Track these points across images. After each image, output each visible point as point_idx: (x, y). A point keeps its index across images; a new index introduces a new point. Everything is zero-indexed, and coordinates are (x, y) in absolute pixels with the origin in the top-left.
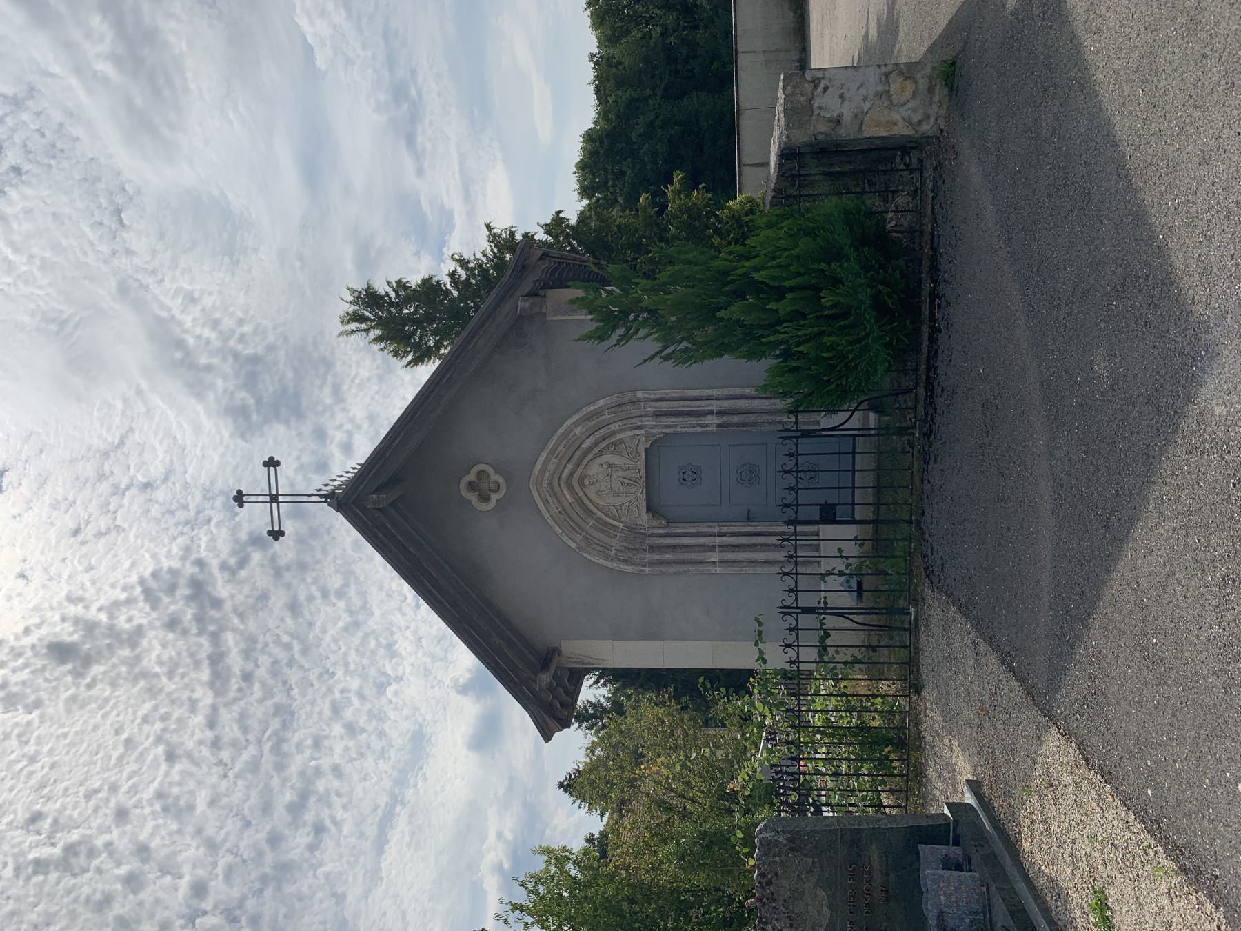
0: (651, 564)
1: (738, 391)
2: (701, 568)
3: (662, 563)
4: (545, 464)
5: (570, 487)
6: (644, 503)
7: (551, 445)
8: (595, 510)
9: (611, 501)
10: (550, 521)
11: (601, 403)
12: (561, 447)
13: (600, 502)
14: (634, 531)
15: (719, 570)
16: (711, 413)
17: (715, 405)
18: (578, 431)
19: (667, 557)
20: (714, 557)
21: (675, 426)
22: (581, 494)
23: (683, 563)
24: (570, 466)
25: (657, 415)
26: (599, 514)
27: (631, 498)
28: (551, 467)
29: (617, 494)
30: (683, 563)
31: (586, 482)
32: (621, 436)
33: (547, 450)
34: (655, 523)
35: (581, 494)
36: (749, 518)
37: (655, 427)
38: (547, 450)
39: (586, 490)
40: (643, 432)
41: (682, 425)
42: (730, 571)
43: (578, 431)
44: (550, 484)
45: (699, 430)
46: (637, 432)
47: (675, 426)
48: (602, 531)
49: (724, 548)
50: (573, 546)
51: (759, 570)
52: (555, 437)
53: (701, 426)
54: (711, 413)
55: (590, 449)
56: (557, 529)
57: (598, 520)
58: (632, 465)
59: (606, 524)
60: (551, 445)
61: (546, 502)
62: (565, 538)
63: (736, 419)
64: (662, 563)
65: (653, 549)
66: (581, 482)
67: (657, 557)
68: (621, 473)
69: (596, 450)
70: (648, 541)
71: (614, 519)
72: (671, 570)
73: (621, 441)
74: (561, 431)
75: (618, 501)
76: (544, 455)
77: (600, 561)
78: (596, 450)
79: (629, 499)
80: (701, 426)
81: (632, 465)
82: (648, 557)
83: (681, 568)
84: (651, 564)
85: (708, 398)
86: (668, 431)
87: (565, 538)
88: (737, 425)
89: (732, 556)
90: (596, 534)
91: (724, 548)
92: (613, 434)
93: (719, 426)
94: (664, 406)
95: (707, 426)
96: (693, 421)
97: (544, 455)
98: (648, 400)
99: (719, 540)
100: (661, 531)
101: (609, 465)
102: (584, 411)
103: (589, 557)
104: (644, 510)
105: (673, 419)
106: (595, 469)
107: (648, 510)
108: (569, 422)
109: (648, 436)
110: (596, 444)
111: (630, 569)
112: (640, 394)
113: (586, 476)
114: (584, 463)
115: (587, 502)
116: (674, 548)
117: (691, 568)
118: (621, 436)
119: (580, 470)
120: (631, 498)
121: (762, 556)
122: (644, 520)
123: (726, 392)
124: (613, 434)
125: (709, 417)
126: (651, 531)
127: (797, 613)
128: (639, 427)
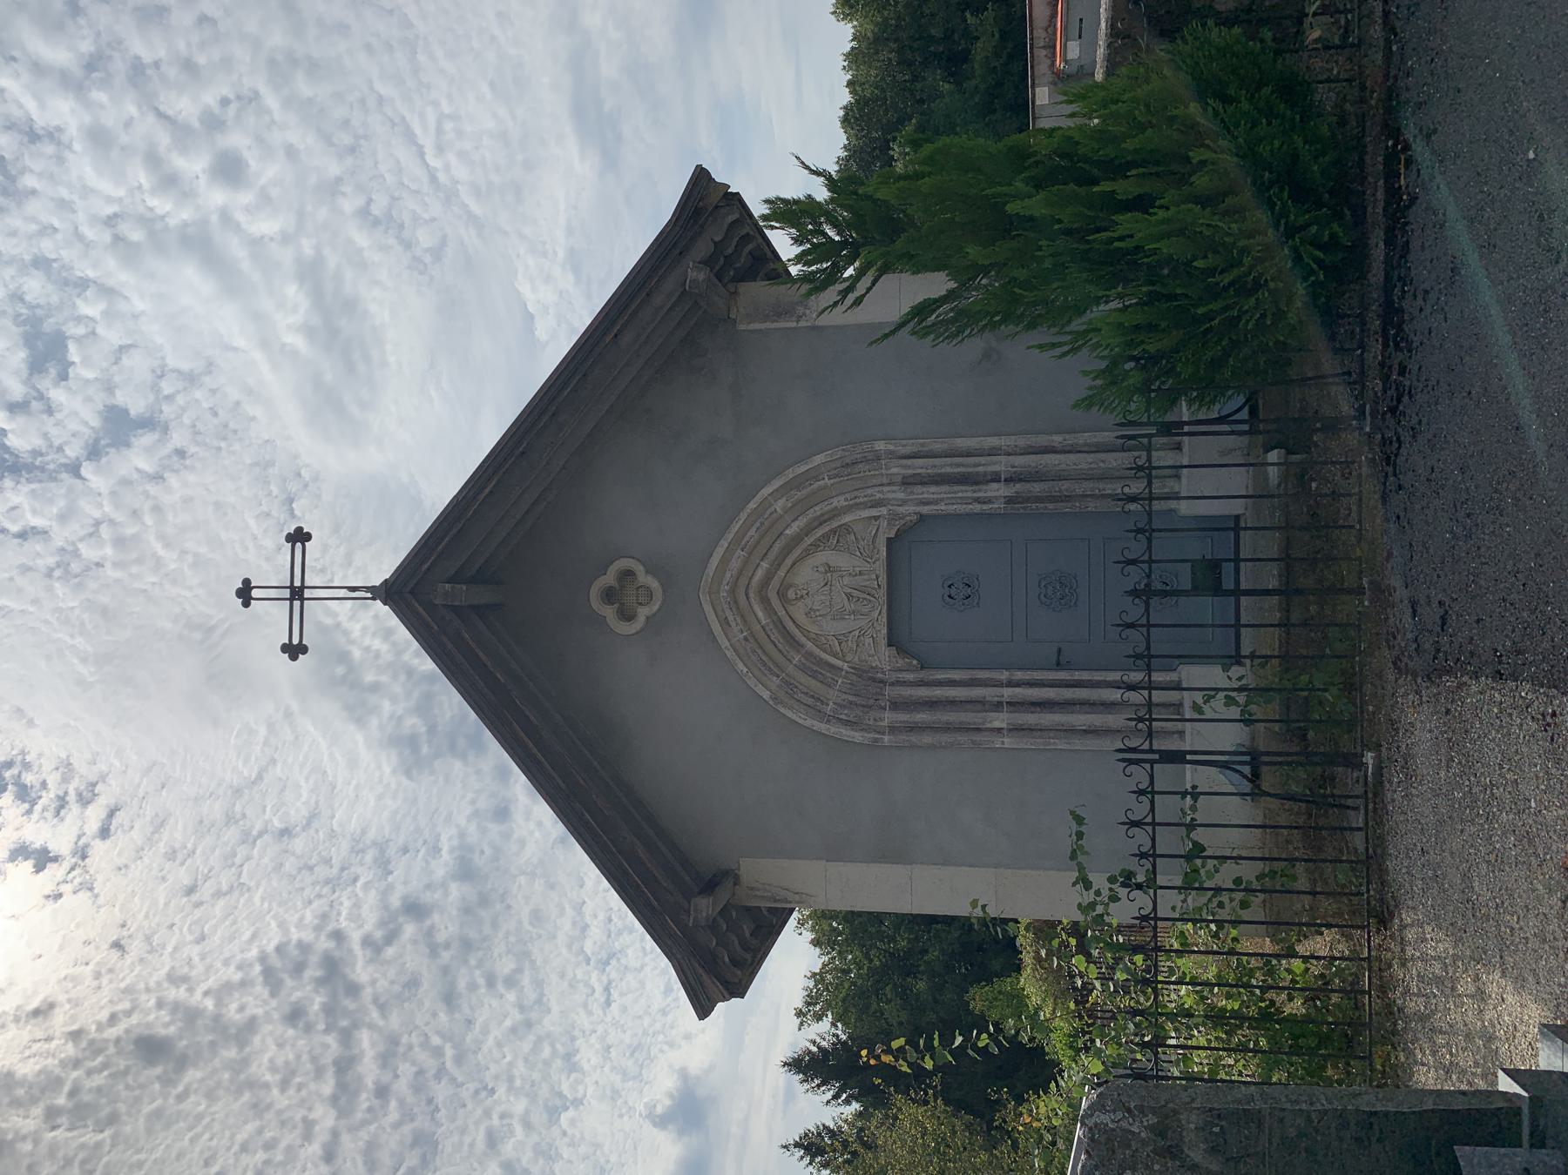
0: (893, 729)
1: (1042, 440)
2: (977, 737)
3: (912, 728)
4: (725, 561)
5: (765, 601)
6: (884, 631)
7: (736, 527)
8: (803, 640)
9: (830, 627)
10: (730, 653)
11: (818, 459)
12: (752, 532)
13: (813, 629)
14: (866, 677)
15: (1008, 742)
16: (996, 478)
17: (1001, 465)
18: (779, 505)
19: (921, 717)
20: (999, 720)
21: (936, 502)
22: (782, 613)
23: (948, 728)
24: (765, 565)
25: (907, 482)
26: (809, 645)
28: (735, 564)
30: (948, 728)
31: (791, 594)
32: (847, 519)
33: (730, 536)
34: (901, 663)
35: (782, 613)
36: (1059, 665)
37: (904, 502)
38: (730, 536)
39: (790, 608)
40: (884, 511)
41: (948, 500)
42: (1025, 743)
43: (779, 505)
44: (733, 592)
45: (977, 508)
46: (874, 512)
47: (936, 502)
49: (1015, 705)
50: (766, 695)
51: (1078, 744)
52: (743, 516)
53: (978, 500)
54: (996, 478)
55: (798, 539)
56: (741, 666)
57: (809, 655)
60: (736, 527)
61: (725, 623)
63: (1037, 488)
64: (912, 728)
65: (895, 706)
66: (782, 595)
67: (904, 717)
68: (846, 581)
69: (809, 540)
70: (887, 690)
72: (927, 739)
73: (847, 528)
74: (752, 505)
76: (724, 543)
77: (809, 723)
78: (809, 540)
80: (978, 500)
82: (888, 717)
83: (945, 738)
84: (893, 729)
85: (993, 452)
86: (925, 510)
87: (752, 682)
88: (1039, 499)
89: (1030, 719)
90: (804, 679)
91: (1015, 705)
92: (836, 513)
93: (1010, 500)
94: (920, 466)
95: (989, 501)
96: (967, 492)
97: (724, 543)
98: (892, 455)
99: (1008, 693)
100: (910, 677)
101: (829, 569)
103: (789, 714)
104: (884, 642)
105: (933, 489)
106: (806, 575)
107: (890, 645)
108: (766, 491)
109: (893, 517)
110: (807, 530)
111: (858, 736)
112: (880, 446)
114: (789, 561)
116: (932, 704)
117: (962, 738)
118: (847, 519)
119: (781, 573)
121: (1081, 720)
122: (882, 658)
123: (1022, 442)
124: (836, 513)
125: (994, 485)
126: (894, 676)
127: (1152, 762)
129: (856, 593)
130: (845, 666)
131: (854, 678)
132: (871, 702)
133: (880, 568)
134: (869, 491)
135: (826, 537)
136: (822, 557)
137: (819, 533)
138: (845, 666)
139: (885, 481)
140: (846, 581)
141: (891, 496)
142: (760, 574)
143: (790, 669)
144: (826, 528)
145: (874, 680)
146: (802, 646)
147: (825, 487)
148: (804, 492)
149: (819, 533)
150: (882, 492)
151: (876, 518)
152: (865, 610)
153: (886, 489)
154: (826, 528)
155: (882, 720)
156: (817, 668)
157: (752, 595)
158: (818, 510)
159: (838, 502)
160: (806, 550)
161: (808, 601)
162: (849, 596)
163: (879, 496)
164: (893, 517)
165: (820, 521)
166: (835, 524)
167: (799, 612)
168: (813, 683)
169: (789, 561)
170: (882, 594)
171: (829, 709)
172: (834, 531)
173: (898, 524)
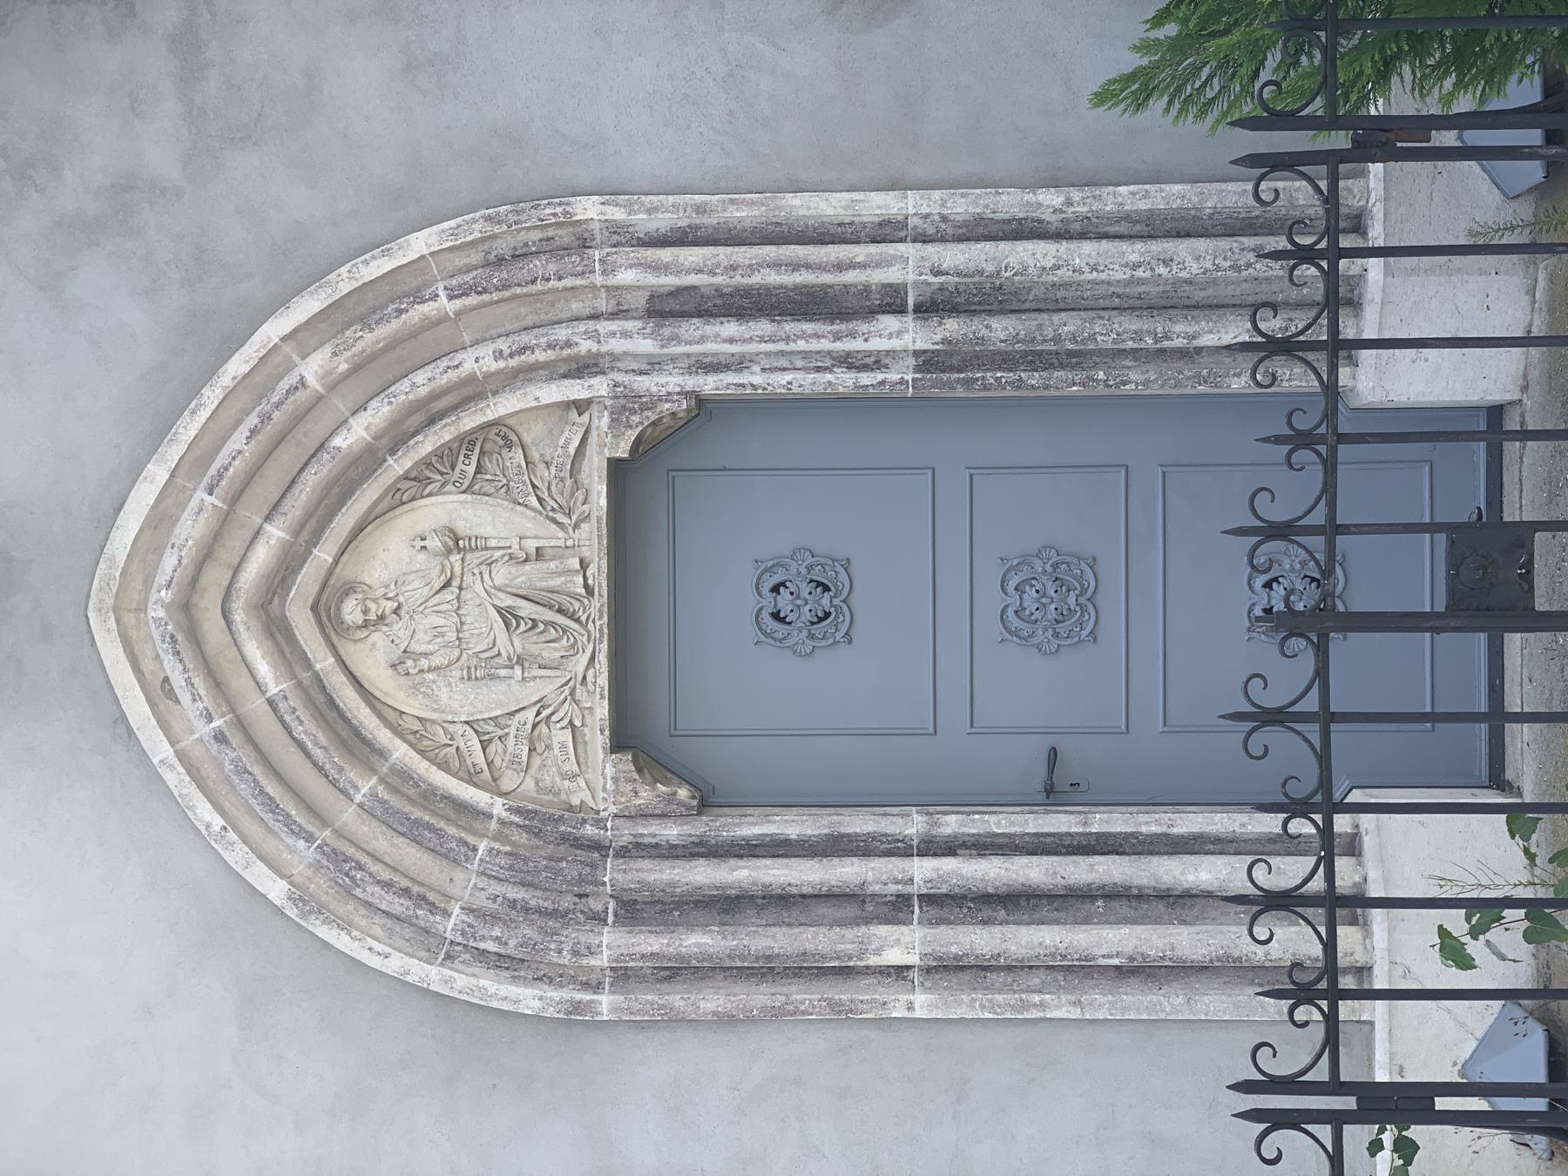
0: (623, 976)
1: (1009, 203)
2: (842, 993)
3: (673, 972)
4: (161, 520)
5: (278, 632)
6: (602, 710)
7: (189, 428)
8: (384, 736)
9: (457, 701)
10: (176, 778)
11: (420, 243)
12: (238, 440)
13: (413, 706)
15: (923, 1002)
16: (891, 302)
17: (905, 266)
18: (313, 368)
19: (697, 941)
20: (901, 945)
21: (739, 364)
22: (324, 662)
23: (765, 970)
24: (276, 533)
25: (666, 308)
26: (401, 752)
27: (545, 687)
28: (190, 529)
29: (485, 669)
30: (765, 970)
31: (351, 611)
32: (503, 406)
33: (173, 453)
34: (646, 796)
35: (324, 662)
36: (1053, 795)
37: (654, 364)
38: (173, 453)
39: (349, 651)
40: (599, 386)
41: (770, 361)
42: (968, 1004)
43: (313, 368)
44: (185, 608)
45: (844, 380)
46: (576, 390)
47: (739, 364)
48: (413, 832)
49: (946, 904)
50: (276, 890)
51: (1102, 1003)
52: (211, 396)
53: (849, 361)
54: (891, 302)
55: (368, 461)
56: (205, 813)
57: (402, 778)
58: (552, 537)
59: (430, 796)
60: (189, 428)
61: (160, 694)
62: (237, 856)
63: (1000, 330)
64: (673, 972)
65: (635, 910)
66: (325, 613)
67: (651, 943)
70: (613, 873)
72: (712, 1000)
73: (501, 434)
74: (237, 366)
75: (488, 700)
76: (158, 473)
79: (534, 691)
80: (849, 361)
81: (552, 537)
82: (611, 944)
83: (760, 996)
84: (623, 976)
85: (887, 232)
86: (709, 384)
87: (237, 856)
88: (1005, 360)
89: (979, 940)
90: (382, 841)
91: (946, 904)
92: (472, 391)
93: (928, 362)
94: (694, 267)
95: (877, 362)
96: (814, 337)
97: (158, 473)
98: (623, 237)
99: (923, 871)
100: (672, 832)
101: (455, 542)
102: (344, 282)
103: (341, 941)
104: (598, 740)
105: (731, 328)
106: (395, 557)
107: (618, 745)
108: (275, 329)
109: (625, 405)
110: (396, 437)
111: (529, 998)
112: (589, 209)
113: (349, 589)
115: (349, 698)
116: (728, 906)
117: (803, 995)
118: (503, 406)
119: (323, 554)
120: (545, 687)
121: (1111, 940)
122: (598, 782)
123: (961, 206)
124: (472, 391)
125: (889, 322)
126: (626, 834)
127: (1337, 1120)
128: (584, 368)
129: (526, 609)
130: (498, 807)
131: (521, 838)
132: (567, 902)
133: (592, 540)
134: (561, 333)
135: (447, 456)
136: (441, 509)
137: (426, 445)
138: (498, 807)
139: (603, 305)
140: (501, 574)
141: (616, 345)
142: (261, 558)
143: (348, 816)
144: (444, 433)
145: (577, 843)
146: (382, 754)
147: (442, 320)
148: (384, 332)
149: (426, 445)
150: (595, 336)
151: (581, 406)
152: (552, 653)
153: (604, 327)
154: (444, 433)
157: (239, 617)
158: (422, 382)
159: (479, 361)
161: (399, 629)
162: (509, 617)
163: (586, 346)
164: (625, 405)
165: (429, 413)
166: (470, 421)
168: (412, 857)
170: (597, 609)
171: (450, 926)
172: (467, 441)
173: (638, 423)
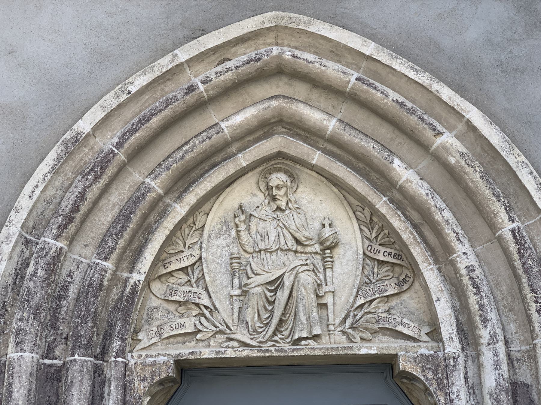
4: (338, 52)
5: (264, 128)
6: (207, 353)
7: (401, 65)
9: (215, 251)
10: (165, 63)
14: (110, 318)
22: (243, 160)
24: (331, 125)
26: (180, 210)
27: (226, 312)
28: (332, 70)
29: (237, 268)
32: (431, 276)
34: (140, 387)
35: (243, 160)
38: (384, 57)
40: (453, 346)
43: (449, 141)
44: (280, 71)
48: (123, 218)
50: (85, 125)
52: (424, 78)
55: (385, 183)
56: (140, 81)
57: (158, 209)
58: (335, 316)
59: (146, 231)
60: (401, 65)
62: (110, 101)
68: (307, 278)
69: (382, 205)
70: (81, 361)
71: (158, 261)
74: (446, 93)
75: (216, 272)
76: (369, 48)
77: (25, 203)
78: (382, 205)
79: (223, 305)
81: (335, 316)
90: (116, 199)
92: (442, 254)
101: (328, 247)
102: (514, 158)
103: (44, 167)
104: (185, 351)
106: (316, 207)
109: (441, 367)
110: (404, 201)
113: (293, 177)
114: (340, 171)
115: (218, 176)
118: (431, 276)
119: (317, 158)
120: (226, 312)
124: (442, 254)
126: (112, 372)
128: (467, 334)
129: (282, 296)
130: (138, 277)
131: (115, 295)
132: (63, 328)
133: (334, 343)
134: (492, 315)
135: (391, 239)
136: (351, 237)
137: (398, 223)
138: (138, 277)
140: (307, 278)
141: (487, 358)
142: (313, 116)
143: (136, 176)
144: (407, 234)
145: (108, 336)
146: (179, 198)
147: (493, 227)
148: (482, 186)
149: (398, 223)
150: (493, 341)
151: (435, 333)
152: (250, 316)
153: (501, 347)
154: (407, 234)
155: (18, 344)
156: (137, 223)
157: (274, 103)
158: (444, 216)
159: (465, 256)
160: (362, 199)
161: (267, 211)
162: (276, 284)
163: (484, 334)
165: (423, 220)
166: (418, 252)
167: (246, 193)
168: (105, 216)
169: (340, 171)
170: (284, 348)
171: (51, 242)
172: (403, 253)
173: (427, 377)
